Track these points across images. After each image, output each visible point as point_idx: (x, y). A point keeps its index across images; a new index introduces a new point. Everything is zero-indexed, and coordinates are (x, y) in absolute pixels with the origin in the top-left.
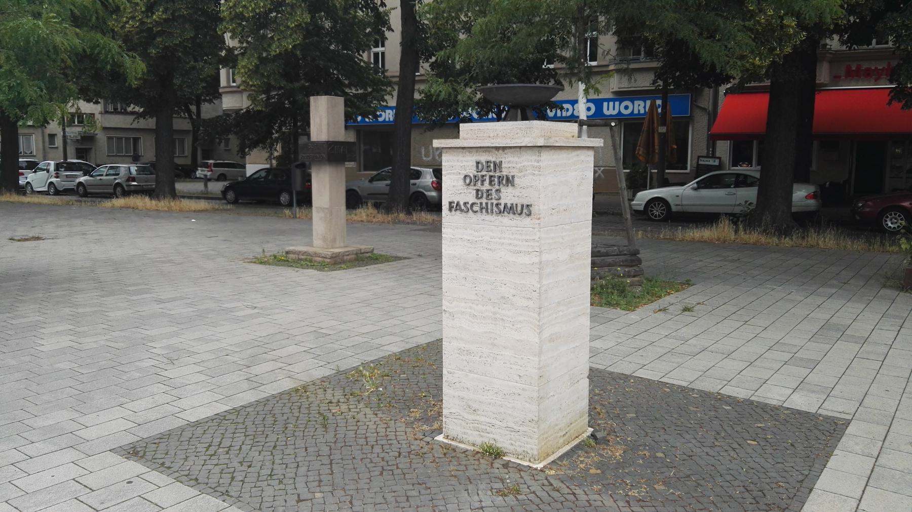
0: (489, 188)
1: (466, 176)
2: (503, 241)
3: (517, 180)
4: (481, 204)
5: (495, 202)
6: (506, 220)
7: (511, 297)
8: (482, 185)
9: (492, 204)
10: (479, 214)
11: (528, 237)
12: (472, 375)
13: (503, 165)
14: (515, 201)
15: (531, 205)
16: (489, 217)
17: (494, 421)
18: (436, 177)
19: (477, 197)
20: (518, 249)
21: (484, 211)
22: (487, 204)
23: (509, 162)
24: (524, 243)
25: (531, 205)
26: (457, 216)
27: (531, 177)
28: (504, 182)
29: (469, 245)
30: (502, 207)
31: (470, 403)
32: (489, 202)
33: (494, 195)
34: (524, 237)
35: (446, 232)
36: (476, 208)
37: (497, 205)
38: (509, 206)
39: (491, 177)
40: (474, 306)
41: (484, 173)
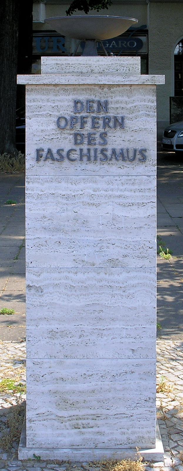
0: (92, 131)
1: (59, 118)
2: (110, 193)
3: (127, 121)
4: (81, 150)
5: (99, 148)
6: (114, 168)
7: (121, 259)
8: (82, 127)
9: (96, 151)
10: (77, 163)
11: (142, 187)
12: (68, 361)
13: (110, 106)
14: (125, 145)
15: (145, 150)
16: (91, 166)
17: (99, 412)
18: (144, 155)
19: (76, 143)
20: (130, 201)
21: (85, 159)
22: (89, 150)
23: (117, 102)
24: (137, 194)
25: (145, 150)
26: (48, 168)
27: (144, 118)
28: (111, 124)
29: (65, 201)
30: (109, 153)
31: (68, 396)
32: (92, 148)
33: (98, 140)
34: (136, 187)
35: (31, 188)
36: (73, 156)
37: (103, 151)
38: (118, 152)
39: (94, 118)
40: (71, 275)
41: (84, 114)
